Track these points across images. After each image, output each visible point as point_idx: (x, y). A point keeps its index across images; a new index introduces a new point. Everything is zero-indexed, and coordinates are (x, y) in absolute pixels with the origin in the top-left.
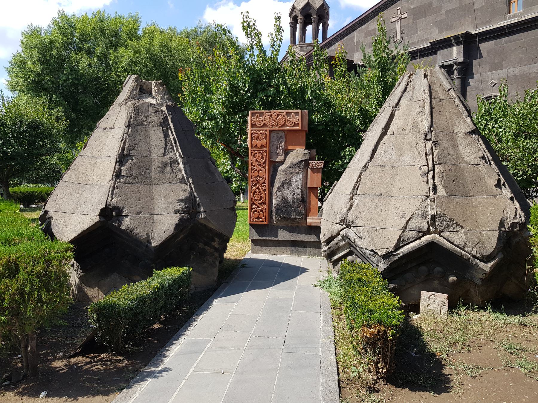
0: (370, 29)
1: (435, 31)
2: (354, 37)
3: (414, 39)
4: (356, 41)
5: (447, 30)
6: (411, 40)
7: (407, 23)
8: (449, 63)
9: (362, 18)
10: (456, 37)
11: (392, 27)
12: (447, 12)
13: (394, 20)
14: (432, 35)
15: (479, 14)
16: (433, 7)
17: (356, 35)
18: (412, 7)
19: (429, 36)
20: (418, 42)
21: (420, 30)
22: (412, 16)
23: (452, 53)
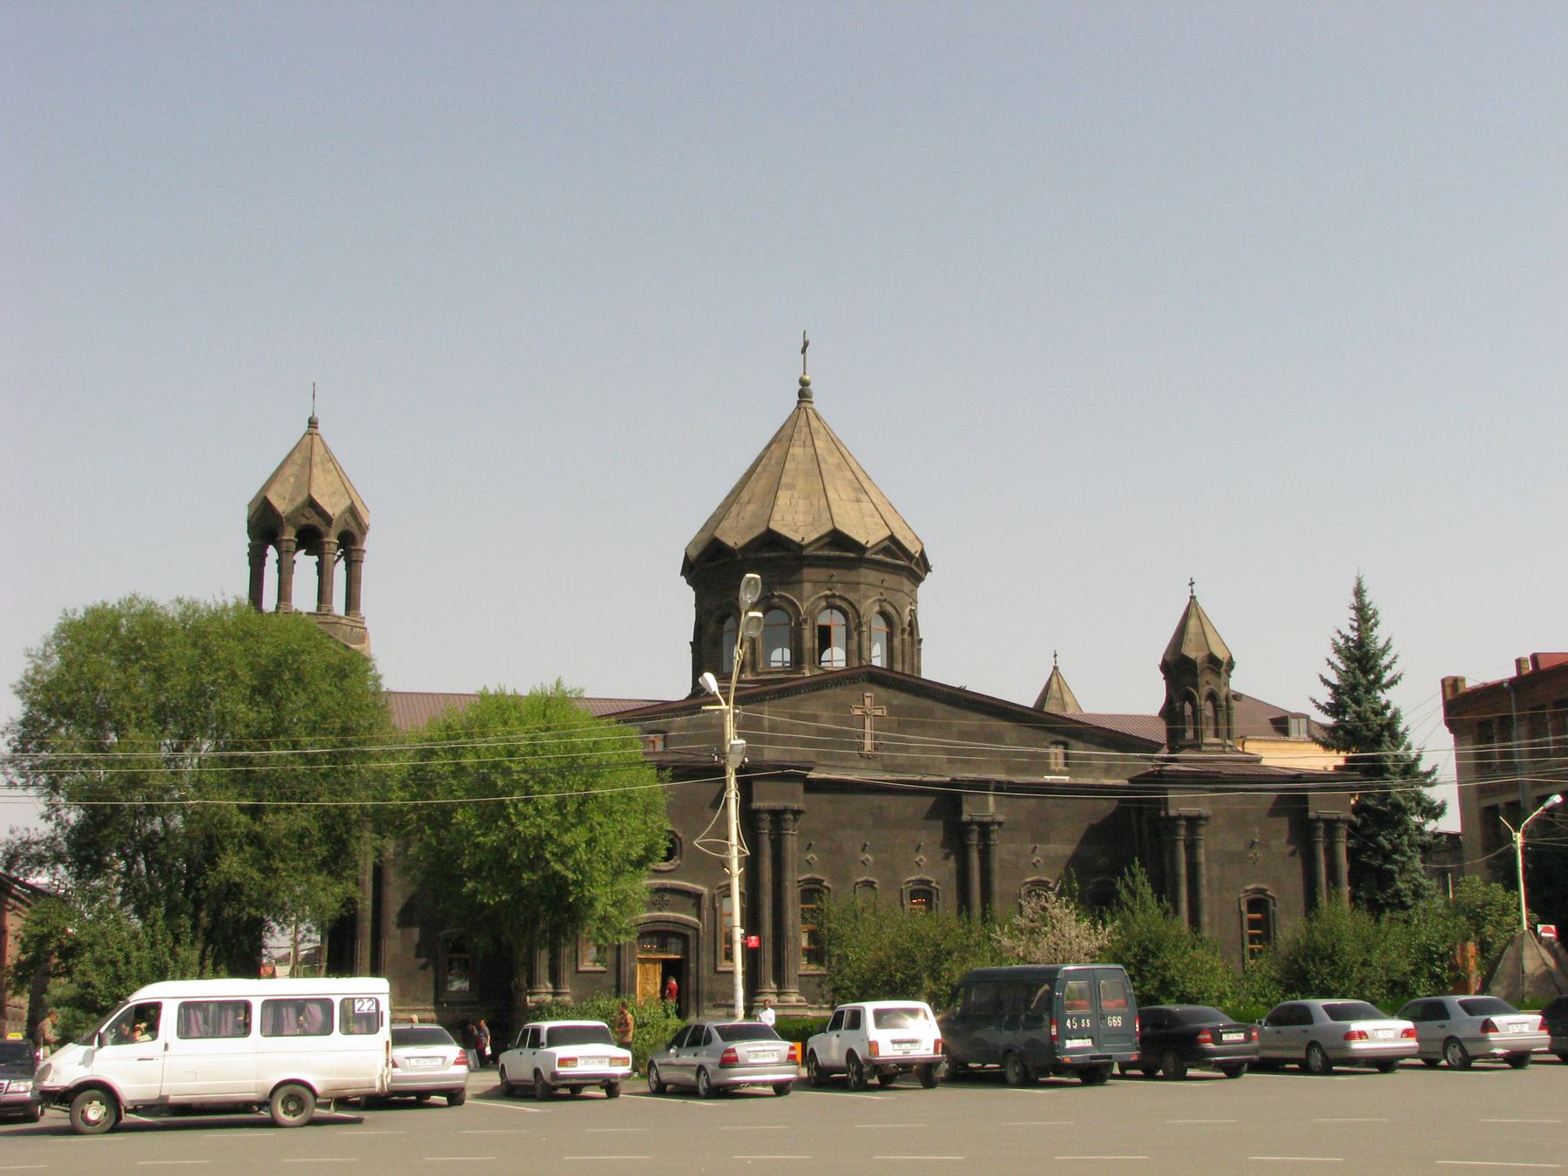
8: (985, 819)
13: (858, 712)
18: (895, 702)
23: (987, 803)
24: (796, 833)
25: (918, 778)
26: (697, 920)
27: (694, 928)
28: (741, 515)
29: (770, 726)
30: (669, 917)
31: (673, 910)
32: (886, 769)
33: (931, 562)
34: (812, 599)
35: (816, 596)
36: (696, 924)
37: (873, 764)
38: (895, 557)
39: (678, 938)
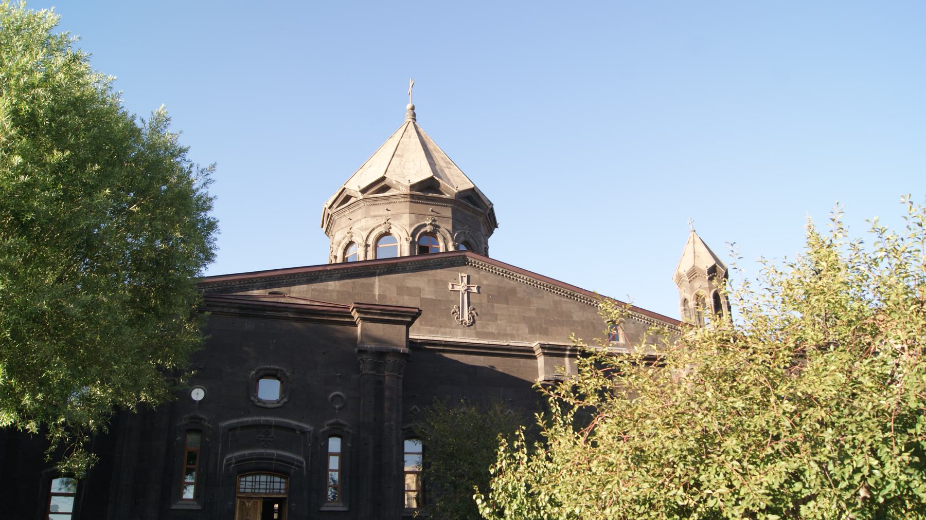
0: (409, 286)
1: (524, 329)
2: (372, 285)
3: (491, 328)
4: (377, 292)
5: (540, 333)
6: (487, 328)
7: (478, 302)
9: (397, 263)
10: (574, 349)
11: (452, 298)
12: (538, 310)
14: (520, 332)
15: (580, 328)
16: (518, 295)
17: (377, 283)
19: (515, 332)
20: (499, 334)
21: (501, 320)
22: (486, 295)
23: (564, 364)
24: (401, 376)
25: (505, 344)
26: (301, 458)
27: (297, 466)
28: (363, 174)
29: (379, 295)
30: (273, 454)
31: (277, 448)
32: (479, 335)
33: (498, 221)
34: (416, 225)
35: (419, 224)
36: (298, 461)
37: (468, 330)
38: (475, 204)
39: (281, 477)
